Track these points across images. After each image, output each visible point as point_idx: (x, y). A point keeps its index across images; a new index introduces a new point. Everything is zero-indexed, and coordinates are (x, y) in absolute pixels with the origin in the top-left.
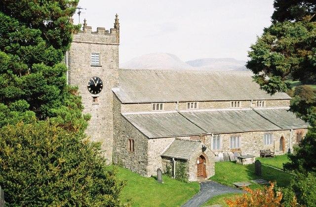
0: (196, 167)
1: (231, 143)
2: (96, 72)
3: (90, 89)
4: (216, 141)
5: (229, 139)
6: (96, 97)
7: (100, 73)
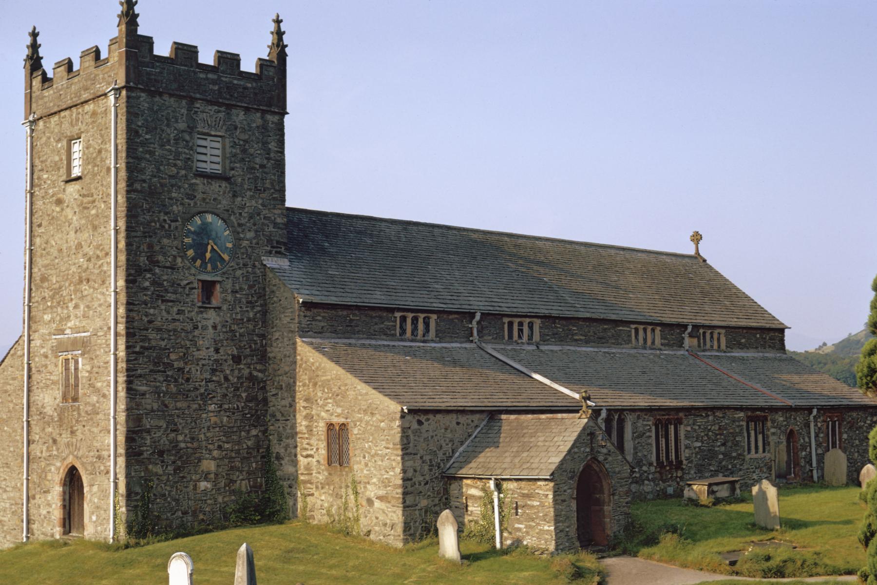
5: (650, 430)
6: (213, 283)
7: (224, 202)
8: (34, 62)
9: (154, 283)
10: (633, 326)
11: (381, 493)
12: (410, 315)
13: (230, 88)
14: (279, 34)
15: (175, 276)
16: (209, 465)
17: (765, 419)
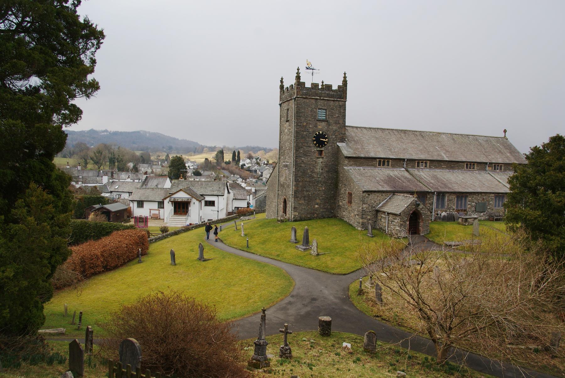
0: (408, 223)
2: (322, 126)
3: (315, 142)
4: (440, 202)
5: (454, 199)
6: (322, 151)
8: (282, 87)
9: (304, 151)
11: (357, 213)
12: (382, 160)
13: (328, 95)
14: (345, 77)
15: (310, 149)
16: (318, 201)
17: (504, 196)
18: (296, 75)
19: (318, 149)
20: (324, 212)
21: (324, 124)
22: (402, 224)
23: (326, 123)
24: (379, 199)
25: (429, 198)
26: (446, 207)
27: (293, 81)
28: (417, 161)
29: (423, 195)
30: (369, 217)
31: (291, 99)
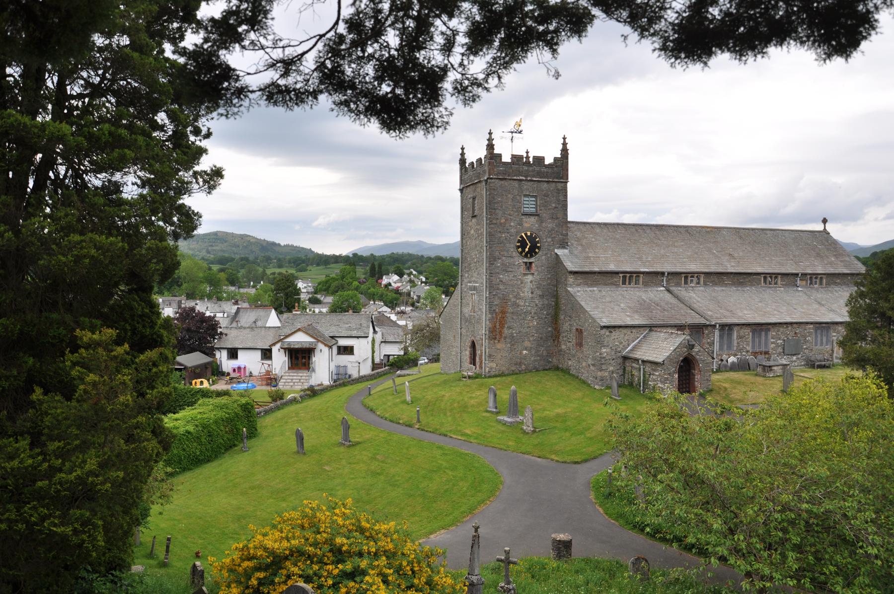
0: (676, 376)
1: (753, 341)
2: (530, 223)
3: (520, 250)
5: (749, 335)
6: (531, 263)
8: (463, 161)
9: (502, 264)
10: (763, 276)
12: (628, 275)
14: (565, 144)
16: (527, 344)
17: (829, 327)
18: (487, 142)
19: (526, 260)
20: (535, 361)
21: (533, 219)
22: (667, 378)
23: (536, 217)
24: (626, 338)
25: (708, 335)
26: (735, 348)
27: (482, 153)
28: (683, 275)
29: (697, 330)
30: (611, 368)
31: (480, 182)
